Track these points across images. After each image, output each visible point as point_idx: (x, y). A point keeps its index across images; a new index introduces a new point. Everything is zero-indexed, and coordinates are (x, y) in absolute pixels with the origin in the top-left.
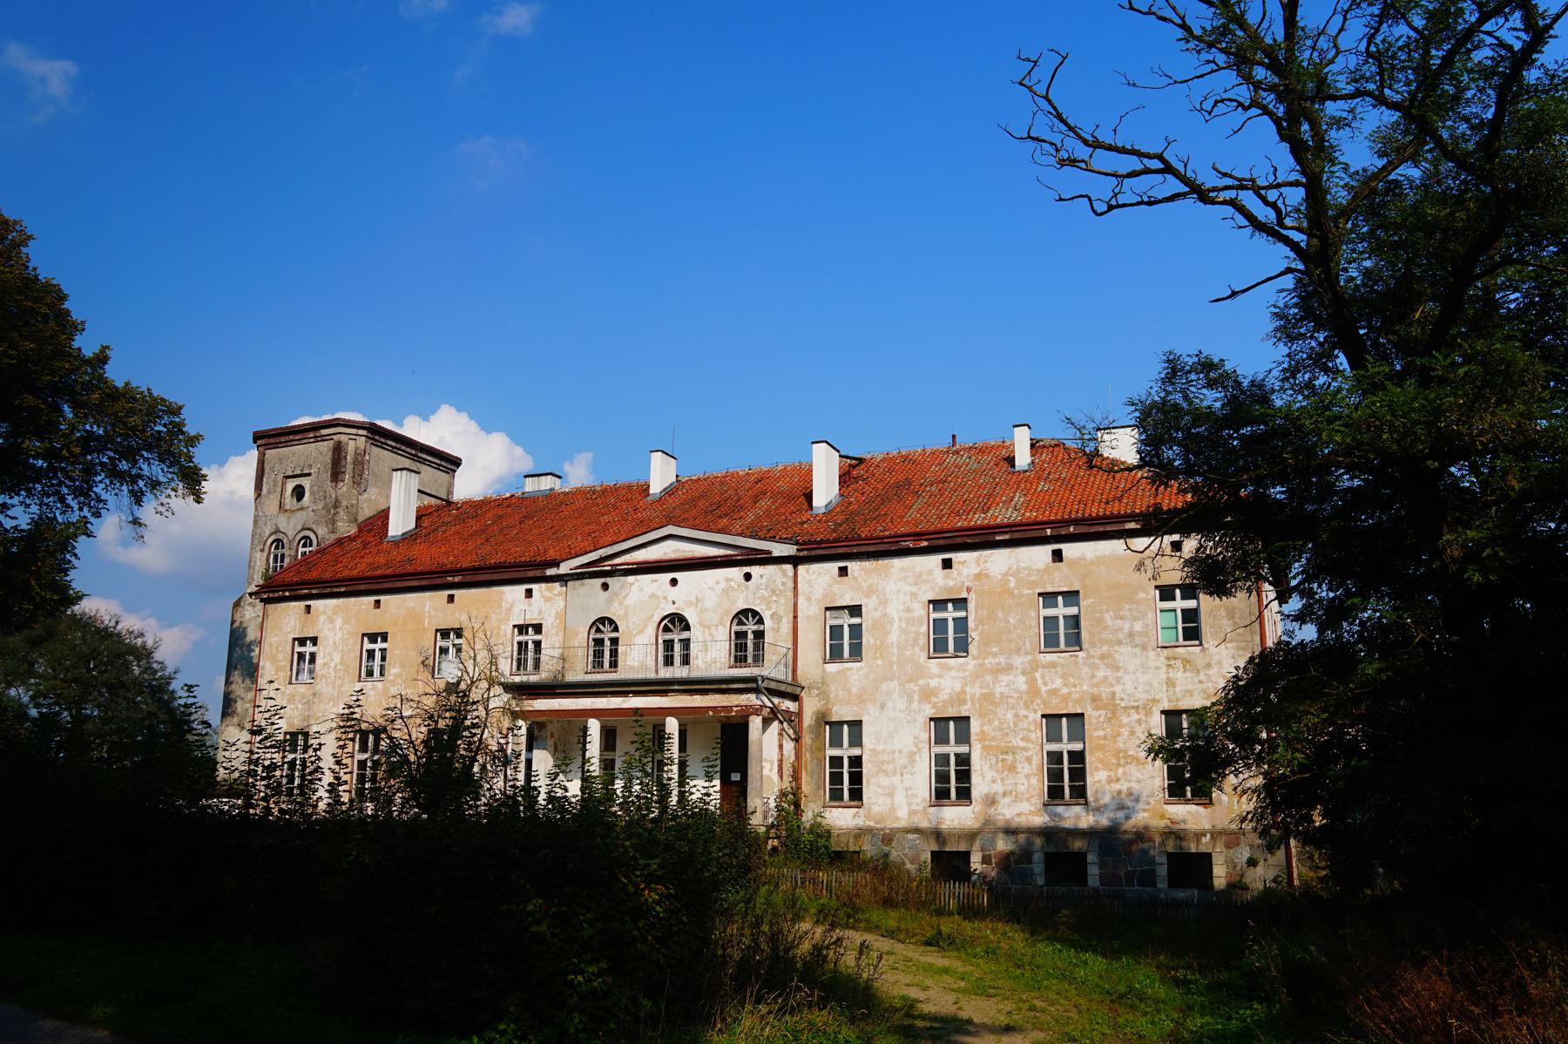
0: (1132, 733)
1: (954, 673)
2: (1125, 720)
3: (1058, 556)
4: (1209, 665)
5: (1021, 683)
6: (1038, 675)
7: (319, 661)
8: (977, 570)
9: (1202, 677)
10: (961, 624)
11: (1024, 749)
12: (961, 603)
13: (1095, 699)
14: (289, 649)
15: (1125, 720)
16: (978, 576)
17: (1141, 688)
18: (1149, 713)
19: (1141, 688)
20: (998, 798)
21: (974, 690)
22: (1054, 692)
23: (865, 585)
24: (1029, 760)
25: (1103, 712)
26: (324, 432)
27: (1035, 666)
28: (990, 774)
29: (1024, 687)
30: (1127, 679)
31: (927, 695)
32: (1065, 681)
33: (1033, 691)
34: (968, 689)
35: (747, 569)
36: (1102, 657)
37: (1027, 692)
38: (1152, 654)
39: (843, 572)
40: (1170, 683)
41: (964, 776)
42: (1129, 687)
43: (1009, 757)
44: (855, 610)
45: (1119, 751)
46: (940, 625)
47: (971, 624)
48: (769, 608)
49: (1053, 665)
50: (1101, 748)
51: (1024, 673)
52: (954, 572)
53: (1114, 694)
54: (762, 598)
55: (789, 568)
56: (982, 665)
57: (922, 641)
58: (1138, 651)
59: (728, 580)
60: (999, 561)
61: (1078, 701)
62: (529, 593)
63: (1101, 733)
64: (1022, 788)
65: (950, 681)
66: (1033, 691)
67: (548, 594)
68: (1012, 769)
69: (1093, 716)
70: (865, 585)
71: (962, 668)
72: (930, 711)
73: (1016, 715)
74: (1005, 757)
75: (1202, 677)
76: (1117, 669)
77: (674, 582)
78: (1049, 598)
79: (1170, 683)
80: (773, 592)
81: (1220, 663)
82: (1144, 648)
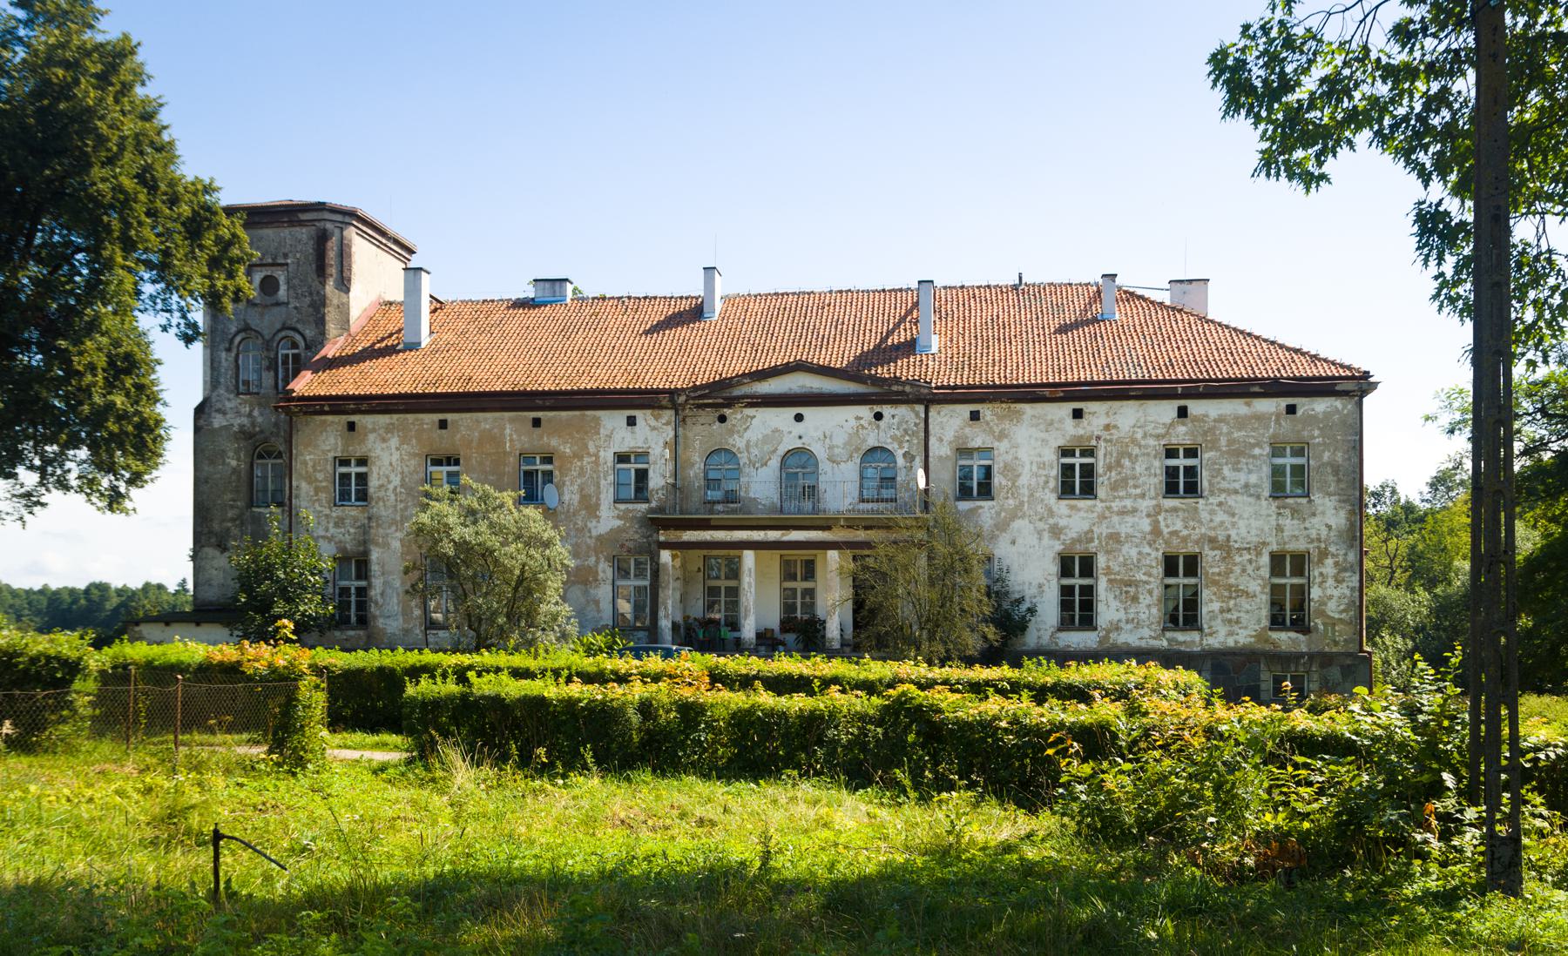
0: (1244, 571)
1: (1082, 514)
2: (1238, 559)
3: (1182, 412)
4: (1314, 515)
5: (1146, 525)
6: (1161, 518)
7: (373, 483)
8: (1107, 421)
9: (1307, 525)
10: (1088, 471)
11: (1147, 583)
12: (1089, 452)
13: (1212, 540)
14: (330, 468)
15: (1238, 559)
16: (1107, 427)
17: (1253, 532)
18: (1259, 554)
19: (1253, 532)
20: (1122, 625)
21: (1102, 530)
22: (1175, 533)
23: (997, 430)
24: (1150, 592)
25: (1217, 552)
26: (304, 217)
27: (1158, 509)
28: (1114, 604)
29: (1148, 528)
30: (1241, 523)
31: (1056, 532)
32: (1183, 524)
33: (1156, 531)
34: (1095, 529)
35: (877, 408)
36: (1220, 504)
37: (1151, 533)
38: (1264, 503)
39: (975, 416)
40: (1279, 529)
41: (1088, 606)
42: (1243, 531)
43: (1132, 590)
44: (987, 451)
45: (1231, 586)
46: (1067, 470)
47: (1100, 469)
48: (901, 447)
49: (1175, 510)
50: (1215, 583)
51: (1148, 516)
52: (1084, 421)
53: (1229, 537)
54: (894, 438)
55: (920, 408)
56: (1109, 508)
57: (1052, 484)
58: (1251, 500)
59: (858, 418)
60: (1127, 415)
61: (1197, 542)
62: (631, 422)
63: (1216, 570)
64: (1143, 617)
65: (1077, 518)
66: (1156, 531)
67: (653, 423)
68: (1135, 599)
69: (1210, 557)
70: (997, 430)
71: (1091, 510)
72: (1058, 547)
73: (1140, 553)
74: (1127, 588)
75: (1307, 525)
76: (1233, 515)
77: (799, 418)
78: (1171, 453)
79: (1279, 529)
80: (906, 431)
81: (1323, 513)
82: (1258, 497)
